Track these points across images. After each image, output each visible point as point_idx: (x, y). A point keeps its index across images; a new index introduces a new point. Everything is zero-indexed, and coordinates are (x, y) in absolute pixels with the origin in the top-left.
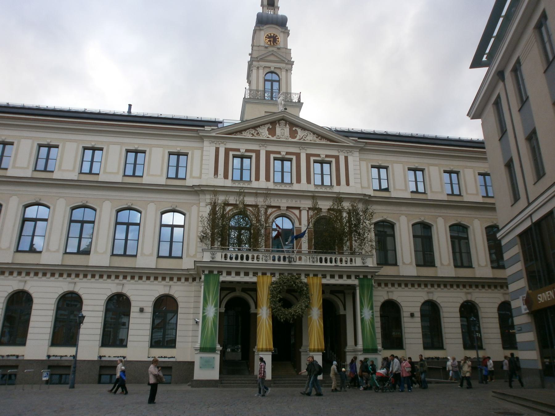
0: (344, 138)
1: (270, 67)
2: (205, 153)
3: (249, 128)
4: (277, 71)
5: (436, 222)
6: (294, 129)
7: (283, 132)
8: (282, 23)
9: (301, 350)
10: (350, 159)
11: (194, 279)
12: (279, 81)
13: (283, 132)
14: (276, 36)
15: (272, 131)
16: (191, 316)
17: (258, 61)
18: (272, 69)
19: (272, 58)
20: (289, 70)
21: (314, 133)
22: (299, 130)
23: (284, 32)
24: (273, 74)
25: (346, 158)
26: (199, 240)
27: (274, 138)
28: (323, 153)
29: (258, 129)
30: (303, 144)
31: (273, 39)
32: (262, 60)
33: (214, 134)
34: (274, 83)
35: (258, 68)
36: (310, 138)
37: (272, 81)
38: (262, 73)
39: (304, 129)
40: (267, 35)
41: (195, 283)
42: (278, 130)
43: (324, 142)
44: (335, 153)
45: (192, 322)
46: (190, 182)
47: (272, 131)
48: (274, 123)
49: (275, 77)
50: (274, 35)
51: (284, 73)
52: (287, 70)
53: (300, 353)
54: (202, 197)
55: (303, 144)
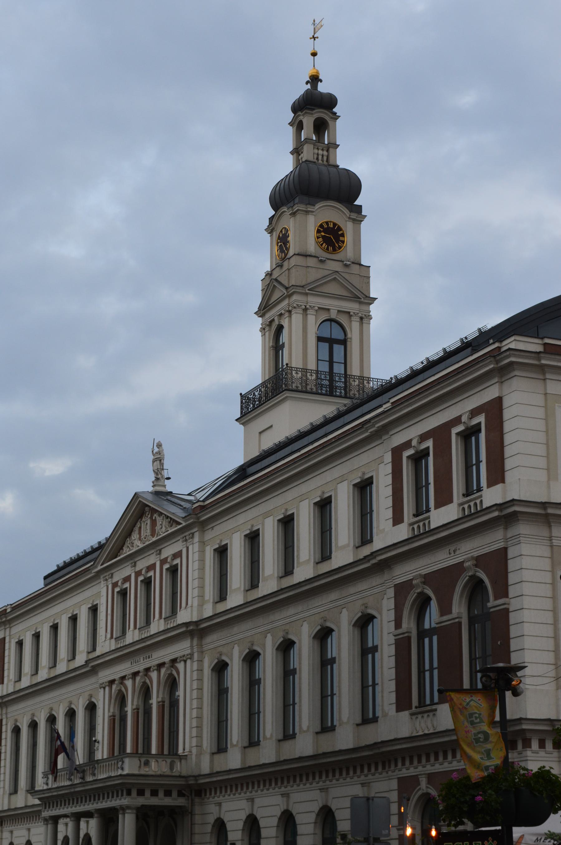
1: (329, 310)
4: (343, 320)
8: (345, 190)
12: (344, 342)
14: (340, 229)
17: (307, 294)
18: (333, 315)
19: (333, 288)
20: (365, 318)
23: (354, 221)
24: (333, 323)
31: (331, 237)
32: (313, 289)
34: (336, 347)
35: (305, 310)
37: (331, 342)
38: (313, 322)
40: (321, 226)
49: (337, 334)
50: (335, 225)
51: (355, 325)
52: (361, 318)
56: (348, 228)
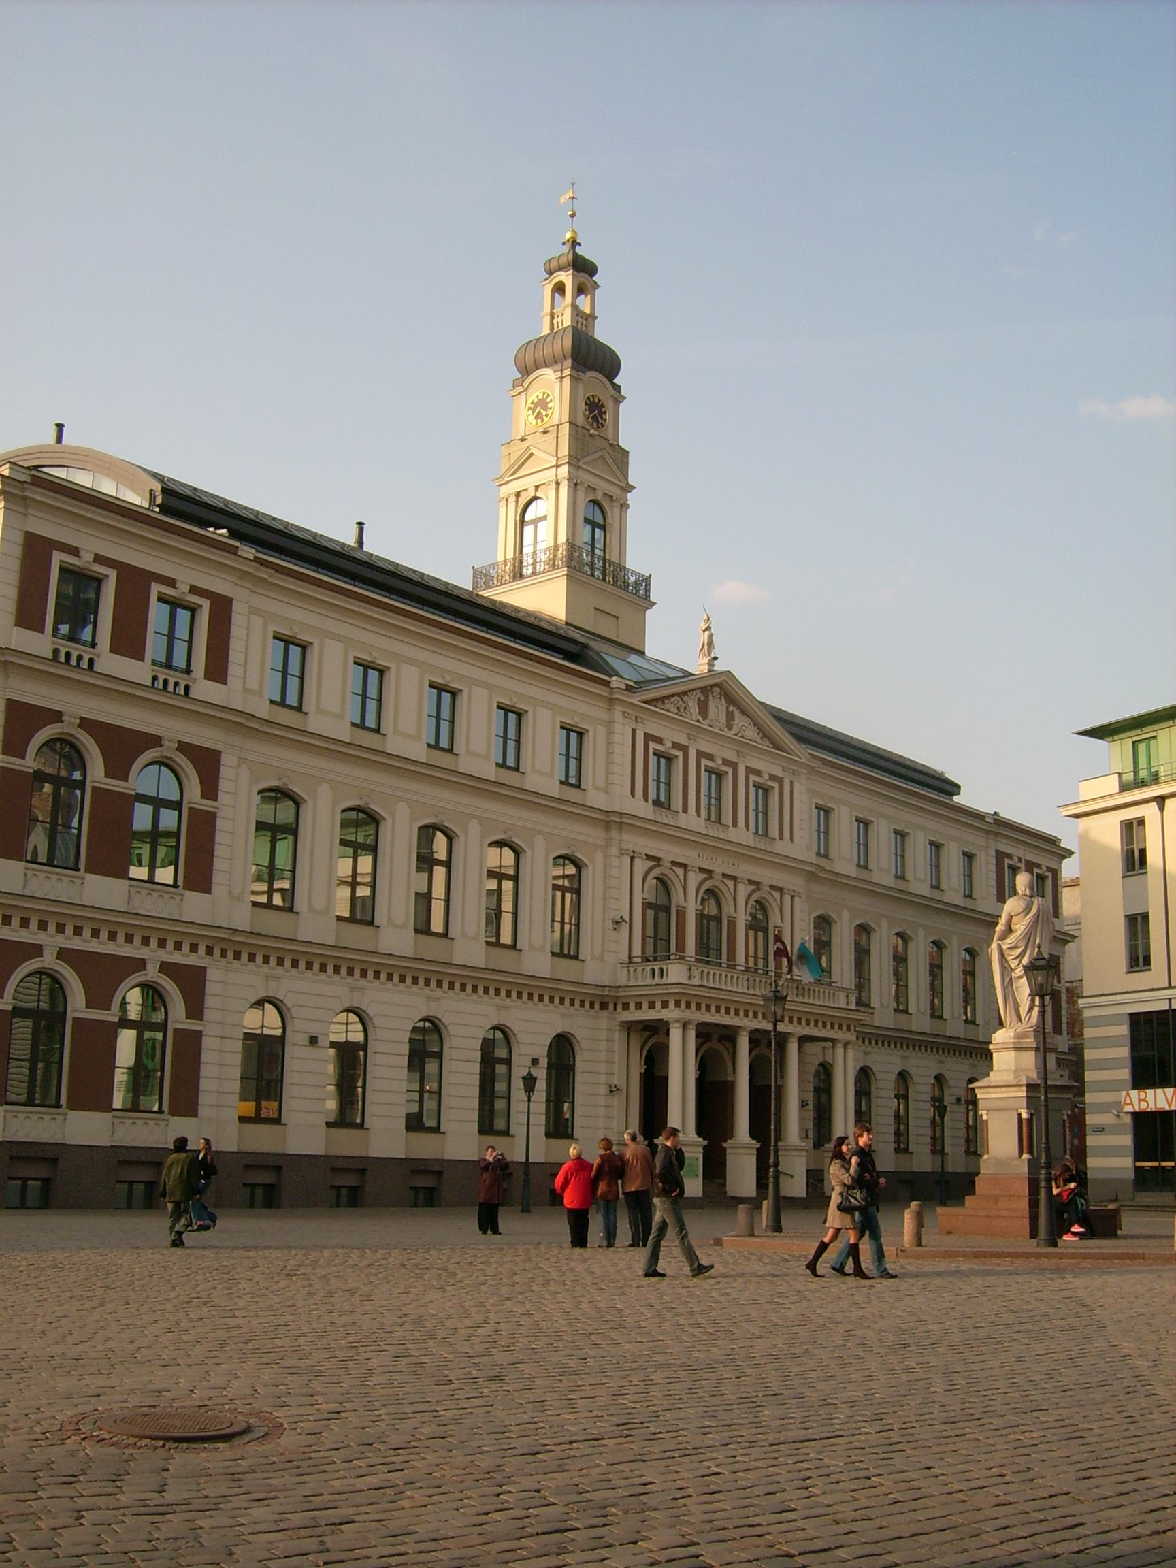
0: (794, 742)
2: (617, 738)
3: (673, 695)
5: (879, 926)
6: (731, 709)
7: (718, 709)
9: (724, 1145)
10: (797, 786)
11: (604, 1006)
13: (718, 709)
15: (703, 710)
16: (602, 1079)
18: (599, 496)
20: (624, 506)
21: (755, 725)
22: (737, 713)
25: (792, 782)
26: (610, 925)
27: (704, 724)
28: (768, 767)
29: (685, 698)
30: (743, 746)
33: (635, 701)
36: (751, 732)
39: (744, 712)
41: (605, 1013)
42: (712, 704)
43: (765, 745)
44: (778, 772)
45: (603, 1090)
46: (594, 798)
47: (703, 710)
48: (706, 690)
51: (617, 511)
53: (725, 1149)
54: (614, 834)
55: (743, 746)
56: (609, 406)
